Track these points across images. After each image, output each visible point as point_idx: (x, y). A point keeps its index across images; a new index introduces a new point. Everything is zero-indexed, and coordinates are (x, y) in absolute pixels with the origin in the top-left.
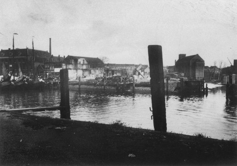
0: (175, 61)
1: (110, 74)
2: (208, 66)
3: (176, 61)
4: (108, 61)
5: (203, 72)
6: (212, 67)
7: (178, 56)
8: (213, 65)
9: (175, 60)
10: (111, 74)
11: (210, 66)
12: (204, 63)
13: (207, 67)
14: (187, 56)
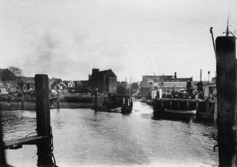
0: (88, 76)
1: (25, 88)
2: (119, 81)
3: (90, 75)
4: (19, 73)
5: (115, 87)
6: (123, 83)
7: (92, 70)
8: (124, 81)
9: (89, 75)
10: (26, 88)
11: (121, 82)
12: (117, 79)
13: (119, 82)
14: (100, 71)
